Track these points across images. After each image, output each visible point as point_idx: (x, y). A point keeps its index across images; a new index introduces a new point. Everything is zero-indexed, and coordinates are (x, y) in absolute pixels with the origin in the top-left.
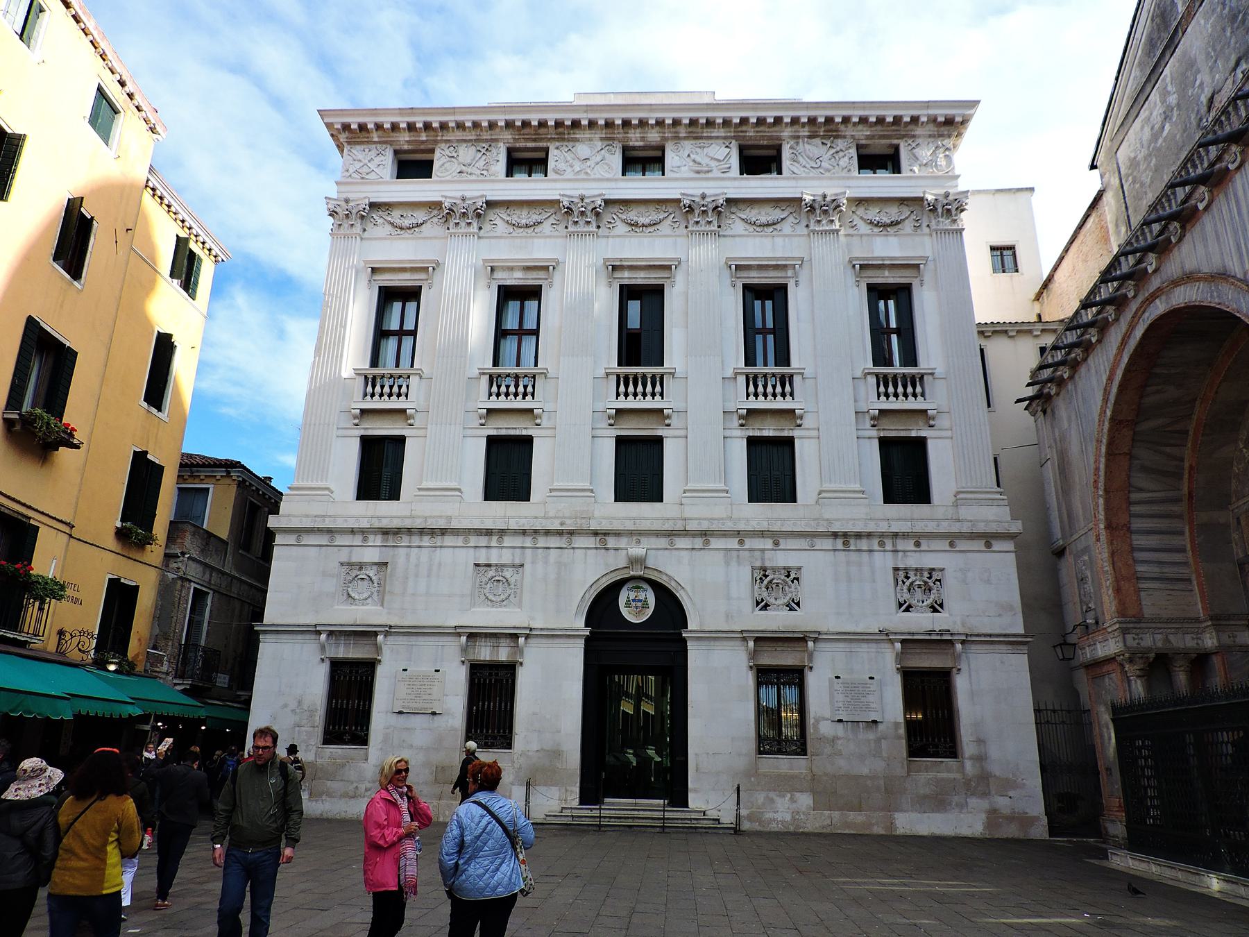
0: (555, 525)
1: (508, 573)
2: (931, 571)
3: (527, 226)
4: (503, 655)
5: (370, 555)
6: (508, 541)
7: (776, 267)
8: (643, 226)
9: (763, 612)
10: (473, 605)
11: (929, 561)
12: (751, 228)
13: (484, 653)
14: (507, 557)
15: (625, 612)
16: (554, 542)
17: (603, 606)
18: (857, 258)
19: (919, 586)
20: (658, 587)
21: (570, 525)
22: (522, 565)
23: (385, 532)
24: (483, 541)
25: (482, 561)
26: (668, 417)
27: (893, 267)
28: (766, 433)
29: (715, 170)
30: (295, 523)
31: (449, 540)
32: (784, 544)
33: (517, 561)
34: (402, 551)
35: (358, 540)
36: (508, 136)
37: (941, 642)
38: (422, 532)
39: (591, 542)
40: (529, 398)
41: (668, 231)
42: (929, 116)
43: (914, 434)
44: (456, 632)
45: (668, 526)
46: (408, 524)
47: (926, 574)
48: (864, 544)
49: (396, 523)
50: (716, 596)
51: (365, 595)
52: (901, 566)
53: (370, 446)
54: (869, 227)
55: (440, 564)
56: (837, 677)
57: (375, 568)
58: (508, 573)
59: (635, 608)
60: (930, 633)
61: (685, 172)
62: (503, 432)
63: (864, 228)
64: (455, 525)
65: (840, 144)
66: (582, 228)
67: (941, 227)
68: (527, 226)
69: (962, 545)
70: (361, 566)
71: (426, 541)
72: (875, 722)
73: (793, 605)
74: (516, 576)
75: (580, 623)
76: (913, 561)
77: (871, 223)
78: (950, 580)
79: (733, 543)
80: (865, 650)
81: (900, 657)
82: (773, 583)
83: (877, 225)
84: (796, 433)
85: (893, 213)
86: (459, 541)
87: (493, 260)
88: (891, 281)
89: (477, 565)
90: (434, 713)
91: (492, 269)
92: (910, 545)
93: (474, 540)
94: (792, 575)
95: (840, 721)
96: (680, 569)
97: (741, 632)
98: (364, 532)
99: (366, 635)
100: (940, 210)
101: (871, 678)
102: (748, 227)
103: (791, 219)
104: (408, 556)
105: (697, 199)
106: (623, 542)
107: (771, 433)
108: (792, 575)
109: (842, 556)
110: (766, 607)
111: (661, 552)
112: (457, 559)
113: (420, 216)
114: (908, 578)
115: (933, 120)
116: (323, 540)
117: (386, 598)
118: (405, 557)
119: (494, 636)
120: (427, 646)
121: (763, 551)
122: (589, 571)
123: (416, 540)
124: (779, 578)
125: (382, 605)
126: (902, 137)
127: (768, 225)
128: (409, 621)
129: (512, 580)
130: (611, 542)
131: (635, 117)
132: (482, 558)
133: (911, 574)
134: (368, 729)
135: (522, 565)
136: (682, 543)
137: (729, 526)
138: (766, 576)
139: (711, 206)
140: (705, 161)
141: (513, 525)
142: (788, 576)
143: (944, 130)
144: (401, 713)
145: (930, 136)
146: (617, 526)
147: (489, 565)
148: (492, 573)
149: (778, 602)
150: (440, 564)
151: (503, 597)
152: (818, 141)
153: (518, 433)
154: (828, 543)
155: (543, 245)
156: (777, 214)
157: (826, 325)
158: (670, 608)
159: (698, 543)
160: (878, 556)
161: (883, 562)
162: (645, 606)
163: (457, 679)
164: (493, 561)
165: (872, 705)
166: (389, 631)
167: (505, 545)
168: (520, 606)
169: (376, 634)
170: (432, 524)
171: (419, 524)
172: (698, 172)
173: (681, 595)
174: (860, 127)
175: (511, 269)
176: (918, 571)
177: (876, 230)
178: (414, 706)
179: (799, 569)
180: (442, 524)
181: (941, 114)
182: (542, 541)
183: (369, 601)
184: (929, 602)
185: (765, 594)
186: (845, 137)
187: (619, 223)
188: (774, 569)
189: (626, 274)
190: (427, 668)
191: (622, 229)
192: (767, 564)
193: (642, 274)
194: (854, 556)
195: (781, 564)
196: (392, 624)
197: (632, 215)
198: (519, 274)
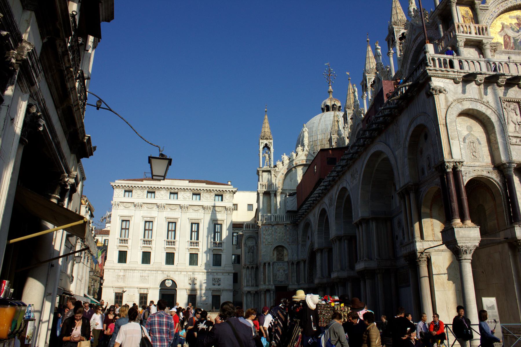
0: (155, 269)
4: (145, 292)
5: (122, 273)
6: (146, 272)
11: (219, 277)
13: (142, 292)
14: (146, 275)
16: (154, 272)
17: (163, 283)
20: (172, 281)
21: (157, 269)
23: (124, 270)
24: (142, 272)
30: (108, 268)
36: (147, 189)
37: (219, 290)
39: (161, 272)
46: (128, 268)
49: (126, 268)
59: (169, 284)
61: (182, 199)
64: (137, 269)
66: (161, 210)
69: (224, 274)
75: (159, 286)
76: (216, 277)
79: (185, 273)
81: (212, 293)
84: (198, 253)
92: (215, 274)
106: (167, 272)
112: (137, 274)
113: (130, 204)
116: (113, 271)
118: (128, 274)
128: (129, 286)
130: (164, 272)
131: (172, 187)
136: (177, 273)
137: (185, 270)
140: (185, 196)
141: (147, 269)
146: (165, 270)
154: (202, 273)
155: (154, 213)
158: (174, 283)
170: (133, 268)
171: (130, 268)
173: (176, 282)
180: (134, 268)
182: (152, 272)
190: (132, 294)
191: (169, 210)
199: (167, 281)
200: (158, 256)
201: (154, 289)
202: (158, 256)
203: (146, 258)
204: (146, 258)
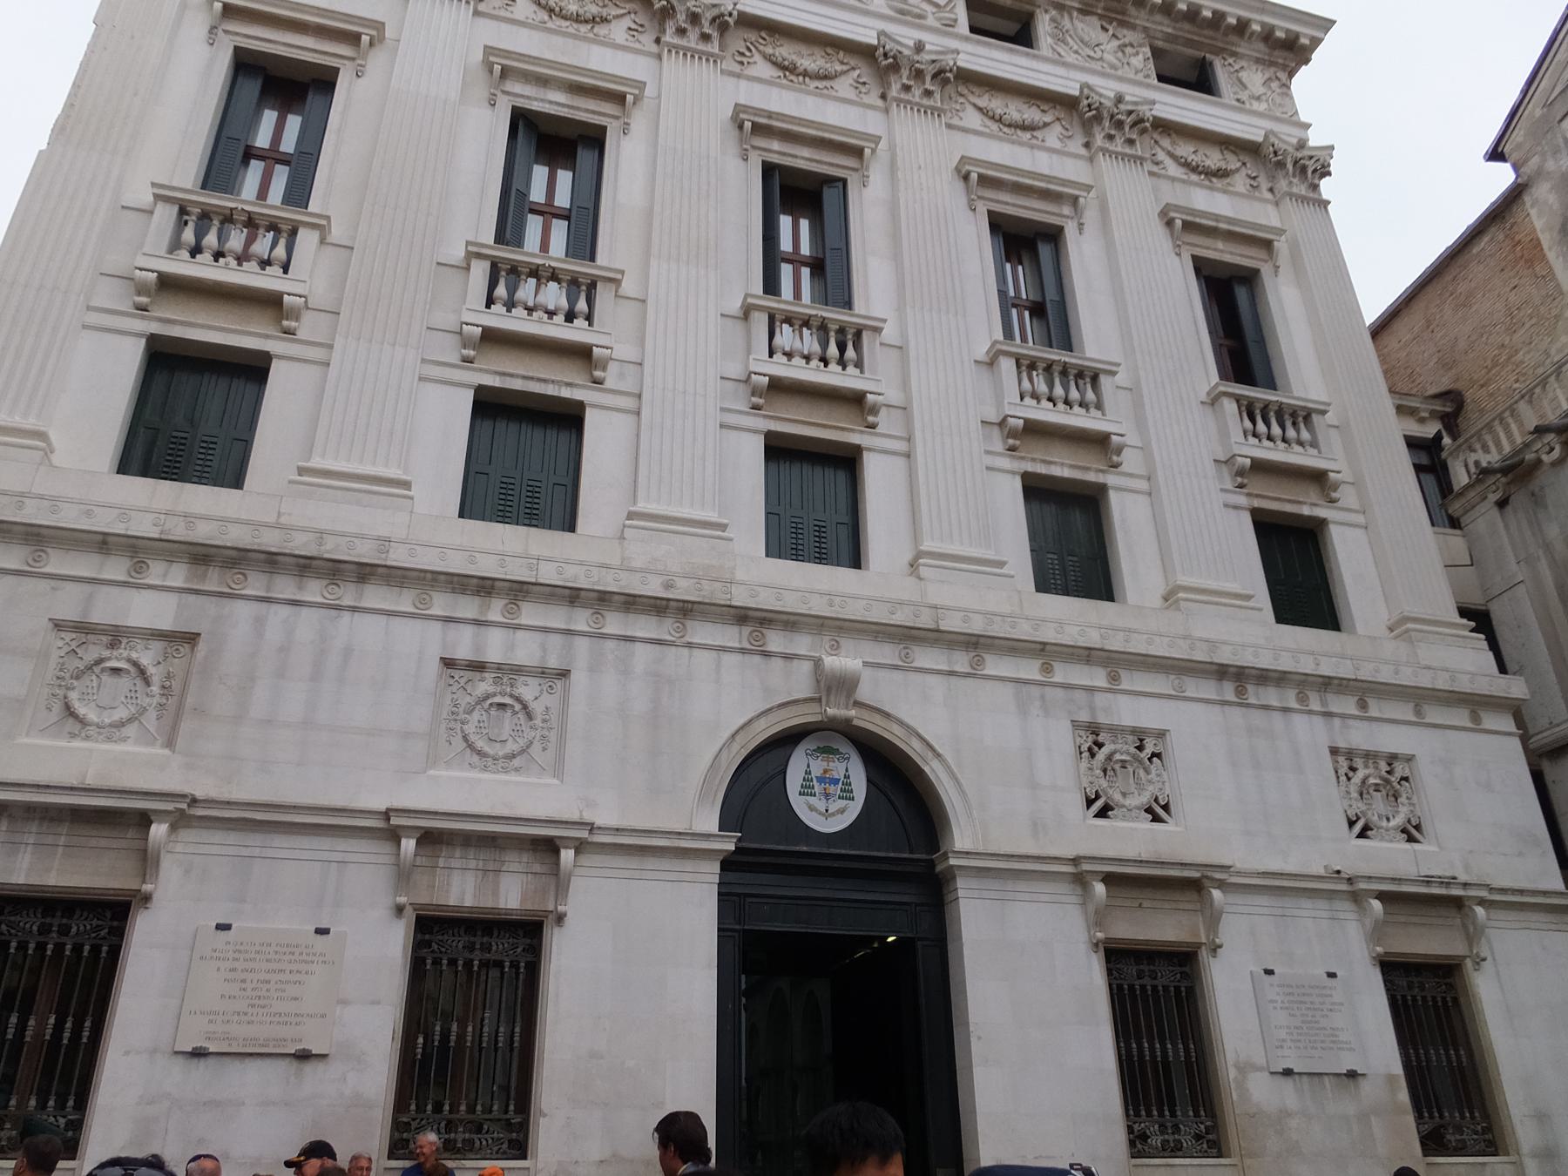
1: (528, 689)
2: (1392, 758)
3: (577, 19)
4: (511, 892)
6: (531, 614)
7: (1045, 195)
8: (805, 74)
9: (1101, 822)
10: (432, 760)
12: (994, 126)
13: (462, 888)
14: (526, 650)
15: (799, 804)
16: (644, 626)
18: (1178, 208)
19: (1377, 788)
22: (564, 674)
24: (467, 607)
25: (463, 652)
26: (874, 410)
27: (1231, 236)
28: (1057, 471)
29: (930, 17)
31: (375, 596)
32: (1129, 681)
33: (553, 663)
34: (244, 610)
35: (116, 568)
38: (305, 566)
39: (730, 635)
40: (580, 322)
41: (851, 94)
42: (1263, 24)
43: (1306, 511)
44: (387, 827)
45: (901, 618)
47: (1384, 767)
48: (1271, 696)
50: (1004, 774)
51: (121, 713)
52: (1342, 744)
53: (166, 362)
54: (1183, 170)
55: (348, 652)
56: (1269, 972)
57: (157, 646)
58: (528, 689)
59: (827, 800)
60: (1427, 881)
62: (517, 385)
63: (1173, 169)
65: (1129, 36)
67: (1295, 190)
68: (577, 19)
70: (116, 635)
71: (314, 590)
72: (1352, 1075)
73: (1157, 812)
74: (546, 700)
76: (1360, 736)
77: (1186, 165)
78: (1428, 774)
79: (1030, 669)
80: (1309, 918)
82: (1119, 762)
83: (1194, 169)
84: (1111, 479)
85: (1213, 158)
86: (404, 601)
87: (507, 54)
88: (1228, 258)
89: (448, 663)
90: (304, 1056)
91: (506, 73)
93: (441, 603)
94: (1147, 748)
95: (1288, 1072)
96: (926, 712)
97: (1075, 861)
98: (137, 549)
99: (119, 820)
100: (1290, 166)
101: (1332, 975)
102: (989, 123)
103: (1057, 128)
104: (259, 622)
105: (906, 52)
106: (802, 644)
107: (1066, 473)
108: (1147, 748)
109: (1236, 714)
110: (1103, 813)
111: (882, 673)
112: (399, 647)
114: (1353, 769)
115: (1267, 36)
117: (186, 725)
119: (486, 842)
120: (295, 867)
121: (1091, 690)
122: (727, 700)
123: (285, 587)
124: (1122, 748)
125: (170, 744)
126: (1219, 51)
127: (1024, 127)
128: (250, 788)
129: (537, 707)
130: (776, 641)
132: (464, 645)
133: (1358, 763)
134: (82, 1103)
135: (564, 674)
136: (926, 657)
138: (1100, 746)
139: (931, 70)
142: (1140, 748)
143: (1280, 56)
144: (198, 1054)
145: (1258, 61)
147: (478, 667)
148: (484, 686)
149: (1132, 801)
150: (348, 652)
151: (511, 747)
152: (1094, 20)
153: (551, 390)
154: (1208, 689)
156: (1032, 114)
157: (1136, 299)
159: (961, 661)
160: (1299, 721)
161: (1309, 734)
162: (847, 794)
163: (380, 953)
164: (493, 655)
165: (1343, 1037)
166: (188, 813)
167: (524, 621)
168: (558, 770)
169: (144, 820)
172: (902, 12)
173: (933, 770)
174: (1158, 17)
175: (543, 81)
176: (1370, 756)
177: (1194, 177)
178: (243, 1034)
179: (1161, 734)
181: (1282, 27)
182: (614, 623)
183: (131, 730)
184: (1398, 821)
185: (1104, 784)
186: (1133, 27)
187: (757, 57)
188: (1116, 731)
189: (776, 145)
190: (296, 924)
192: (1102, 719)
193: (805, 152)
194: (1257, 717)
195: (1128, 721)
196: (199, 793)
197: (785, 51)
198: (560, 97)
199: (800, 765)
200: (672, 463)
201: (640, 849)
202: (672, 463)
203: (525, 447)
204: (525, 447)
